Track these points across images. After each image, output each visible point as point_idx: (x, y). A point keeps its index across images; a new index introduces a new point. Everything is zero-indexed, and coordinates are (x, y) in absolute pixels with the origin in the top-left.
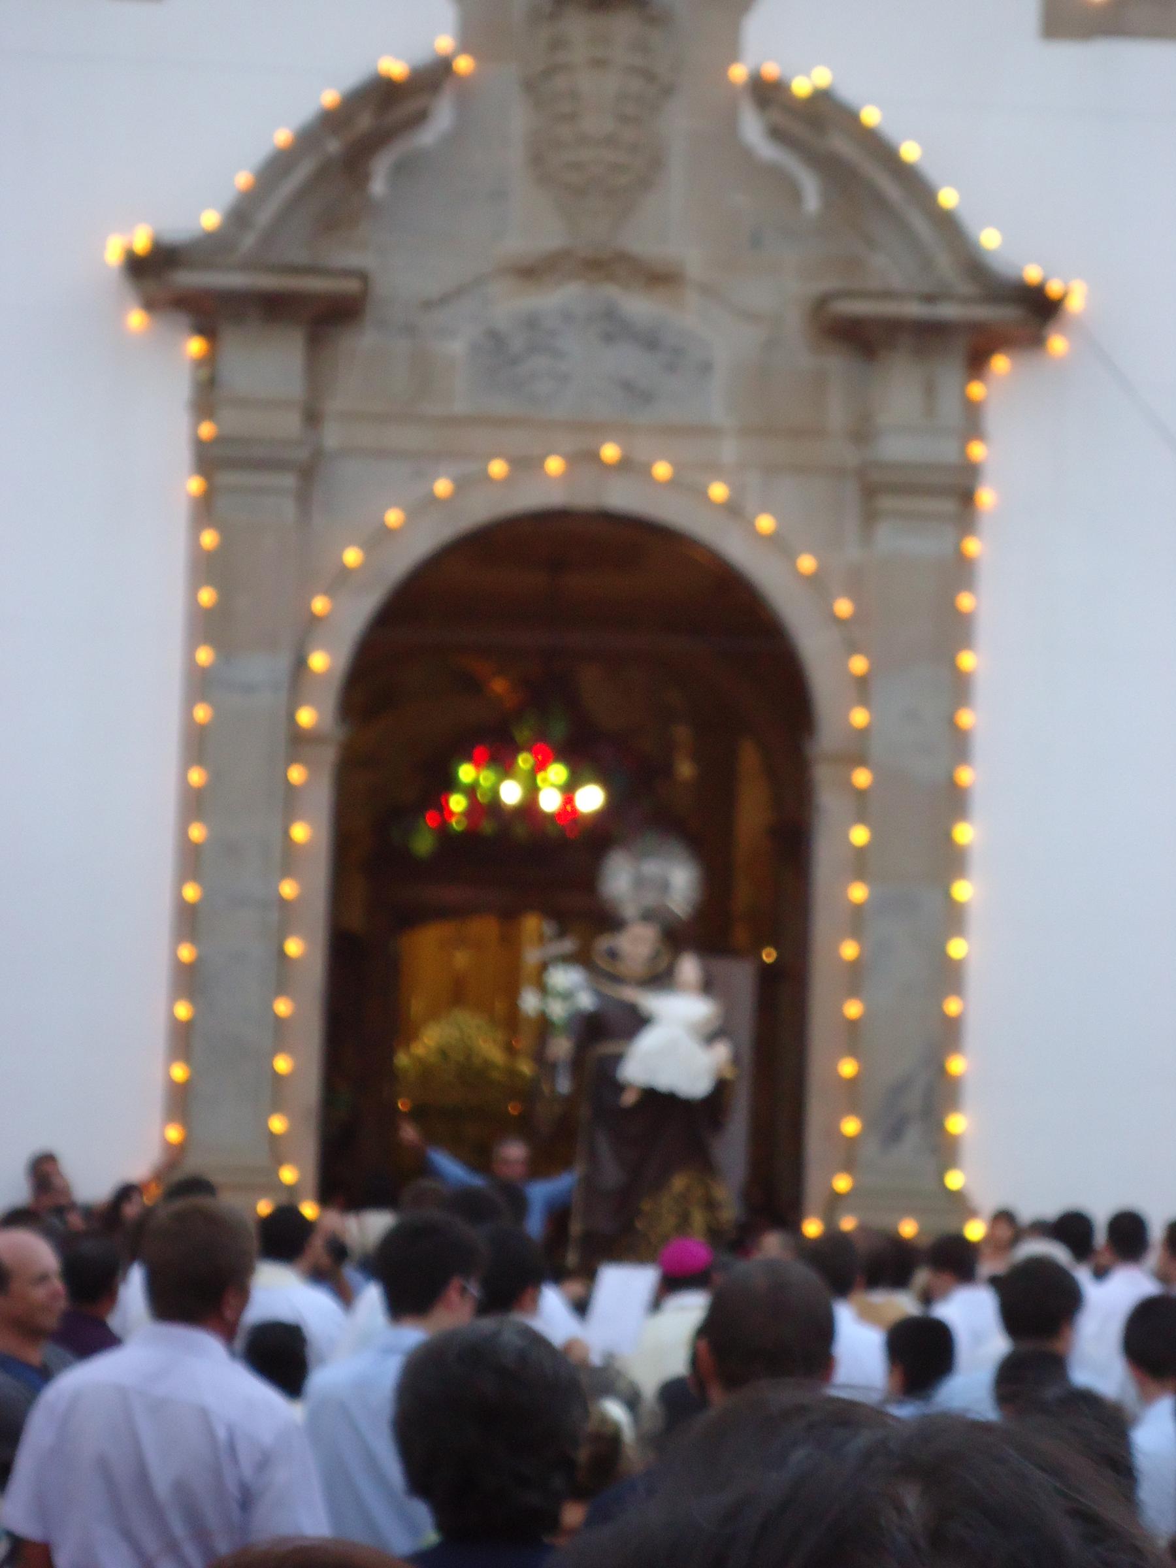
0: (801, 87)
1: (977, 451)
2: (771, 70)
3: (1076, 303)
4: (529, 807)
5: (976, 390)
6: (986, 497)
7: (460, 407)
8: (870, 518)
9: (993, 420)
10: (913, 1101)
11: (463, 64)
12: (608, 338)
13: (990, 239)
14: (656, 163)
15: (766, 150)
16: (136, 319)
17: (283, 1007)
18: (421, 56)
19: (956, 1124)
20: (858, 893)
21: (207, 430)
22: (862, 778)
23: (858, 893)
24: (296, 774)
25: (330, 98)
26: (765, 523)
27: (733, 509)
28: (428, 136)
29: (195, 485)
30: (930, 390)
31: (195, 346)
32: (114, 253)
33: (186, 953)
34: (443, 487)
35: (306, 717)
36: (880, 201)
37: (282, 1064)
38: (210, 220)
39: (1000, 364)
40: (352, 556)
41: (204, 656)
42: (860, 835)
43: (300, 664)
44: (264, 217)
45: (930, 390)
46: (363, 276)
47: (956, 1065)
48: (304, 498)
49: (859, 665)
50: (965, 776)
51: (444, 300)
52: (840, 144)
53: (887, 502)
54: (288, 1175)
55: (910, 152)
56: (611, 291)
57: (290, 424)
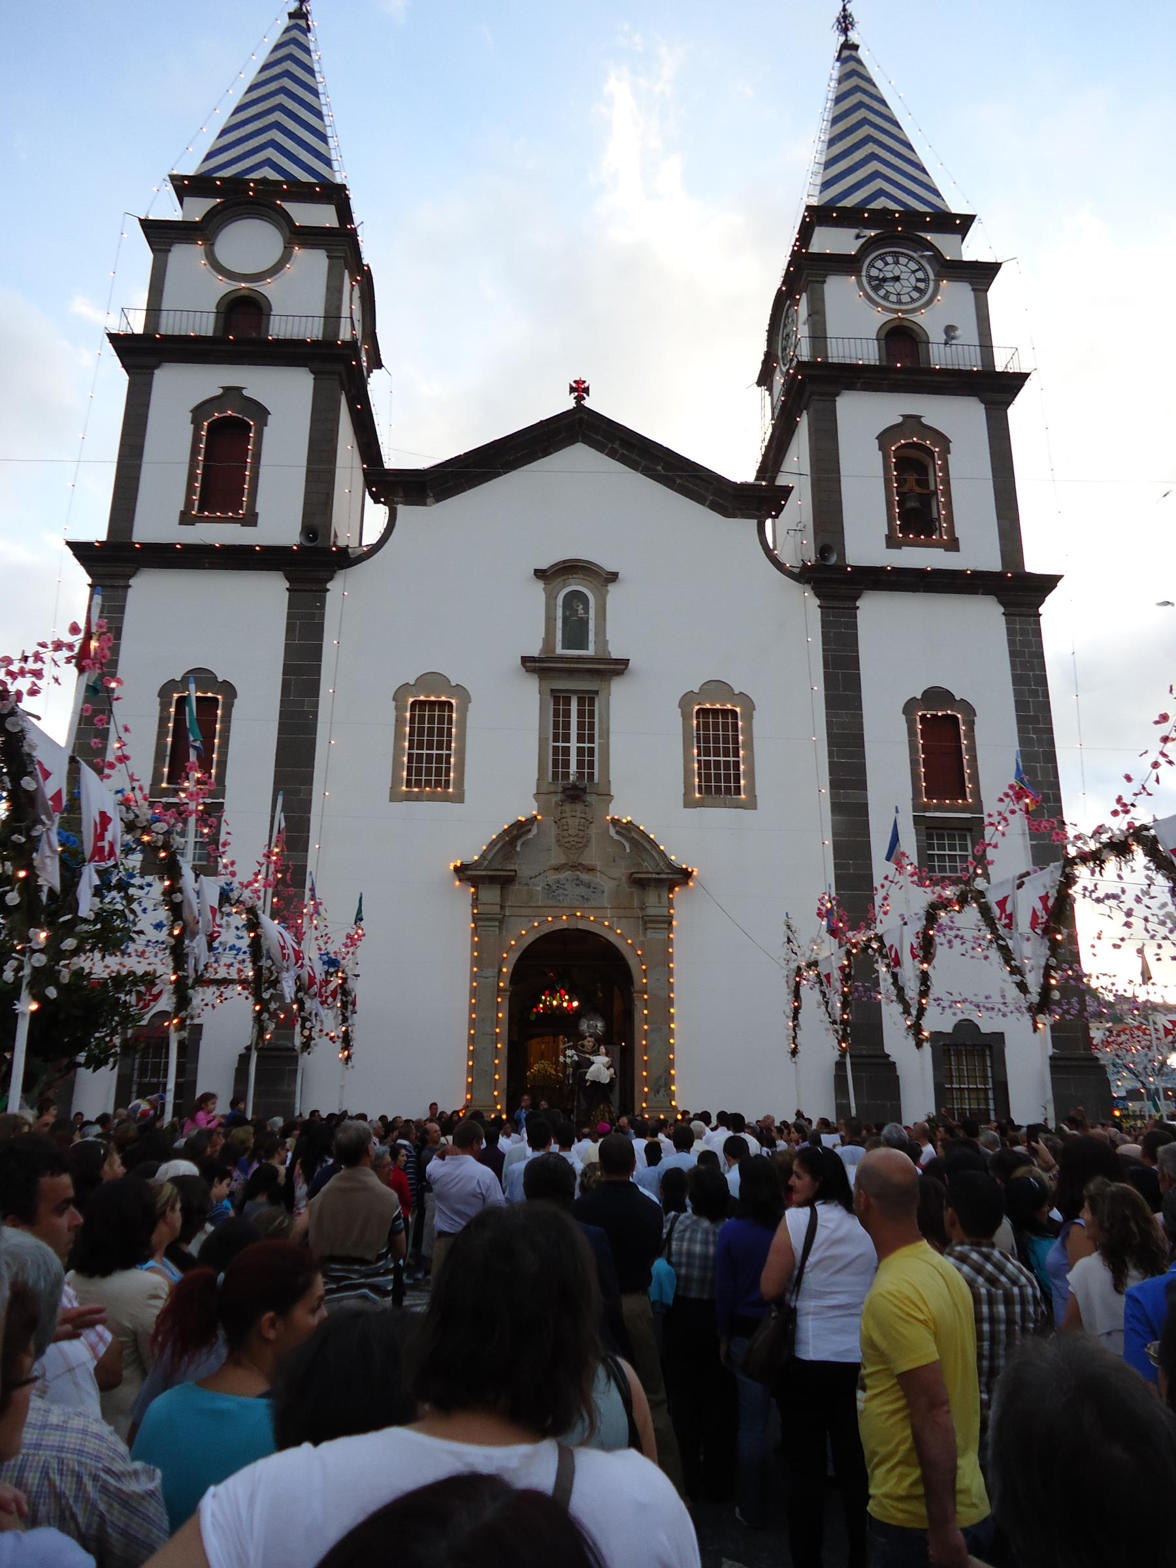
0: (624, 821)
1: (672, 911)
2: (616, 817)
3: (695, 873)
4: (560, 1006)
5: (671, 896)
6: (674, 923)
7: (540, 904)
8: (646, 929)
9: (675, 904)
10: (662, 1082)
11: (539, 817)
12: (577, 885)
13: (673, 858)
14: (588, 841)
15: (616, 837)
16: (457, 883)
17: (497, 1061)
18: (529, 816)
19: (673, 1088)
20: (646, 1027)
21: (475, 911)
22: (646, 997)
23: (646, 1027)
24: (499, 1000)
25: (506, 827)
26: (619, 931)
27: (609, 927)
28: (530, 836)
29: (473, 925)
30: (659, 896)
31: (473, 890)
32: (452, 868)
33: (471, 1048)
34: (536, 924)
35: (501, 984)
36: (646, 849)
37: (497, 1077)
38: (476, 858)
39: (677, 889)
40: (513, 943)
41: (475, 969)
42: (646, 1012)
43: (501, 970)
44: (489, 858)
45: (659, 896)
46: (515, 871)
47: (673, 1072)
48: (500, 928)
49: (644, 967)
50: (672, 995)
51: (536, 876)
52: (634, 834)
53: (649, 925)
54: (499, 1107)
55: (652, 836)
56: (578, 873)
57: (497, 909)
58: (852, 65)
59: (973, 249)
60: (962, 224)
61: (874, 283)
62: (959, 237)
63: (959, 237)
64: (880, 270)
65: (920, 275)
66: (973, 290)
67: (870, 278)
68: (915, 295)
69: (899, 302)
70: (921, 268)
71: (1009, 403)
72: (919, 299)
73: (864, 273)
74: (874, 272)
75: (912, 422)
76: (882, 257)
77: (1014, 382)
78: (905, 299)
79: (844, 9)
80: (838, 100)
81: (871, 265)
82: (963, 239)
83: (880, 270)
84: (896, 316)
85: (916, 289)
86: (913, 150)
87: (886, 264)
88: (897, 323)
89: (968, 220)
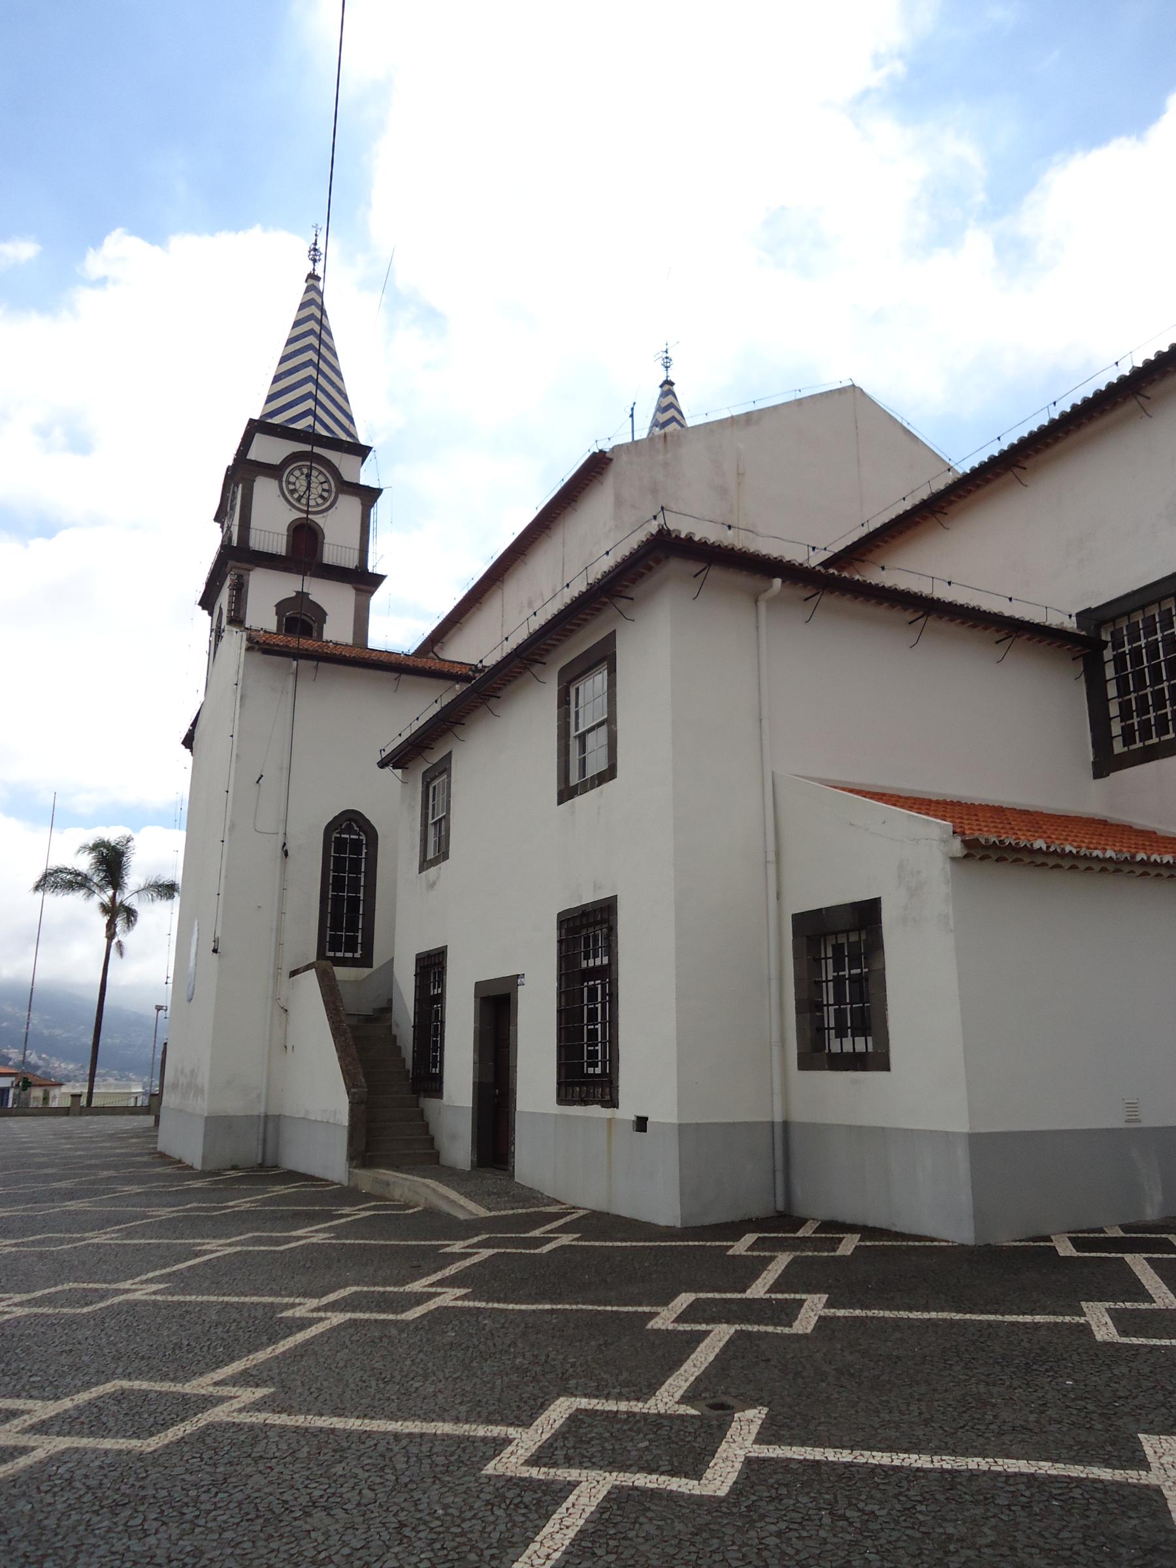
58: (313, 295)
59: (367, 476)
60: (363, 452)
61: (291, 487)
62: (361, 459)
63: (360, 459)
64: (297, 478)
65: (326, 486)
66: (362, 504)
67: (289, 483)
68: (320, 501)
69: (308, 505)
70: (327, 481)
71: (372, 593)
72: (323, 504)
73: (284, 479)
74: (292, 479)
75: (302, 596)
76: (300, 468)
77: (377, 580)
78: (312, 503)
79: (315, 244)
80: (296, 324)
81: (291, 473)
82: (362, 463)
83: (297, 478)
84: (305, 516)
85: (321, 496)
86: (342, 379)
87: (302, 474)
88: (305, 521)
89: (370, 449)
